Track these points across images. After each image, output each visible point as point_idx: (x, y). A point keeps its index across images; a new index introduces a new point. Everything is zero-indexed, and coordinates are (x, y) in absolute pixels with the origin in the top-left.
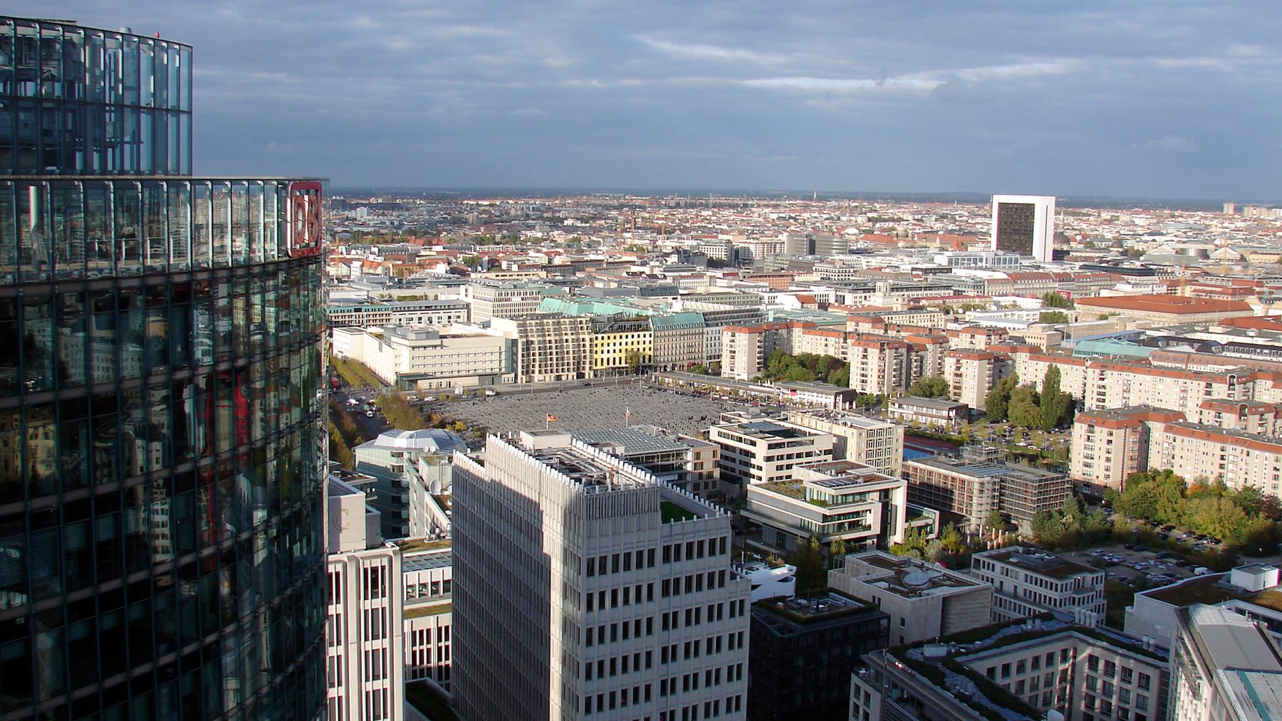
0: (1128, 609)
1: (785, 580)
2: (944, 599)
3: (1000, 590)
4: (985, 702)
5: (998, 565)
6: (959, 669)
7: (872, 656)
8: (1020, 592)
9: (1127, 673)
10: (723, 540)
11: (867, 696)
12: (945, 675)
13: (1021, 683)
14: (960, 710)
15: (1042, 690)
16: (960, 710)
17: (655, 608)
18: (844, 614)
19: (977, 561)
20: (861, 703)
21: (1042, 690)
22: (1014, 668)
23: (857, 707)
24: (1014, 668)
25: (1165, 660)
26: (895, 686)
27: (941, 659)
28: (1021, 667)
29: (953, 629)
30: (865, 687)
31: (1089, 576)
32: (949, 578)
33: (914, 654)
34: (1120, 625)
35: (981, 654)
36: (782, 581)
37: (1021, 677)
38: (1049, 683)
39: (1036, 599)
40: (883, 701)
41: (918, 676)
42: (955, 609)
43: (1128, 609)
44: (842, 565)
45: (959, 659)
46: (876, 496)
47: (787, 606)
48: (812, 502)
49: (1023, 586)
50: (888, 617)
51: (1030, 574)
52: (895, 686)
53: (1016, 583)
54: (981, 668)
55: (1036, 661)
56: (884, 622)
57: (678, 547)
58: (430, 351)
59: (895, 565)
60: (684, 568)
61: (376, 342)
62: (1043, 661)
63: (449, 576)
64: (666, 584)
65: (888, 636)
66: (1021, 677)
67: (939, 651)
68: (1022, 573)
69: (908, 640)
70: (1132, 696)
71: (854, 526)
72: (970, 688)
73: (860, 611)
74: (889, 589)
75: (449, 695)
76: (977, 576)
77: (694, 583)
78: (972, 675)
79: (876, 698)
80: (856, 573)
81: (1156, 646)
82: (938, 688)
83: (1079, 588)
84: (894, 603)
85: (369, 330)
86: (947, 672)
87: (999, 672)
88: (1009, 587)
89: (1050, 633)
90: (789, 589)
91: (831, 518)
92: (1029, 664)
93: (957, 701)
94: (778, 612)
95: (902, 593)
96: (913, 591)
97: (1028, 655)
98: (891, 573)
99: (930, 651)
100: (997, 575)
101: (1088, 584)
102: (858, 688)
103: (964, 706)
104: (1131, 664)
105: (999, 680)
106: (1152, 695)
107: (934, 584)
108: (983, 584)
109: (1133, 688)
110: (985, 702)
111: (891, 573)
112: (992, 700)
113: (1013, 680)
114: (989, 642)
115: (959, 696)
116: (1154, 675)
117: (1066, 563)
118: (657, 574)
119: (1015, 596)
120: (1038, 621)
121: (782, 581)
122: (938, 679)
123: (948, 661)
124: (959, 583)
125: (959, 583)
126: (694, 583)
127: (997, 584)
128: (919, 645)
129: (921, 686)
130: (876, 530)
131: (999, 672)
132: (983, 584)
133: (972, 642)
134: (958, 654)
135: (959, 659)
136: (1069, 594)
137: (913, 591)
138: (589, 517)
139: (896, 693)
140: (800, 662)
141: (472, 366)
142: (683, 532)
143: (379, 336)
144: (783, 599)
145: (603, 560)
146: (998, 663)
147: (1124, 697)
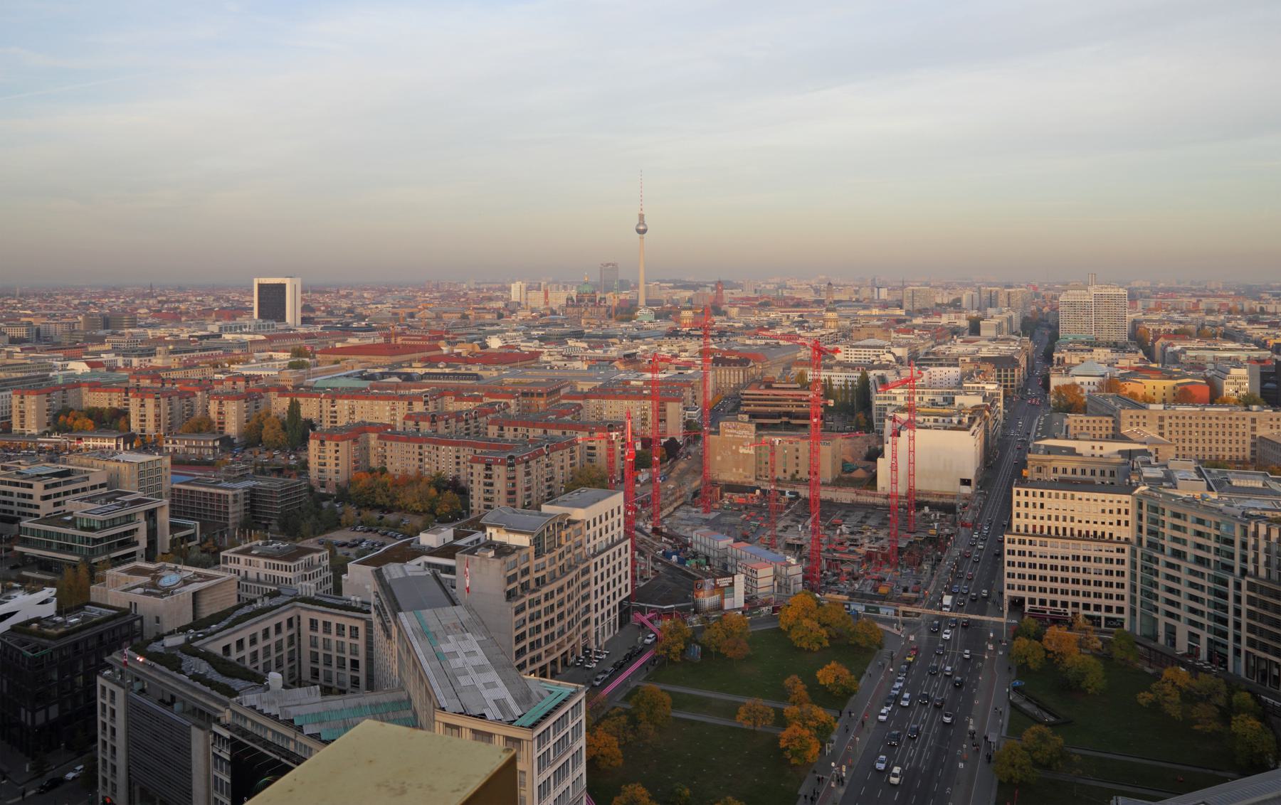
0: (344, 576)
2: (195, 595)
3: (246, 578)
4: (217, 677)
5: (243, 558)
6: (195, 653)
7: (116, 656)
8: (262, 577)
9: (340, 628)
11: (113, 693)
12: (181, 660)
13: (255, 655)
14: (195, 689)
15: (274, 655)
16: (195, 689)
18: (97, 623)
19: (225, 557)
20: (107, 702)
21: (274, 655)
22: (247, 642)
24: (247, 642)
25: (368, 612)
26: (138, 680)
27: (182, 648)
28: (253, 641)
30: (109, 686)
31: (316, 556)
32: (199, 575)
33: (156, 647)
34: (338, 589)
35: (217, 635)
36: (42, 603)
37: (255, 648)
39: (275, 580)
40: (126, 695)
41: (158, 666)
43: (344, 576)
44: (103, 579)
45: (196, 644)
46: (141, 517)
47: (41, 626)
48: (83, 529)
50: (141, 618)
51: (268, 561)
52: (138, 680)
53: (258, 570)
54: (216, 648)
56: (138, 623)
59: (152, 571)
65: (141, 634)
66: (255, 648)
67: (180, 640)
68: (262, 561)
71: (123, 544)
72: (204, 667)
73: (114, 617)
74: (145, 593)
76: (225, 570)
78: (207, 656)
79: (120, 693)
80: (116, 584)
81: (363, 602)
82: (174, 674)
84: (148, 605)
86: (184, 657)
87: (233, 648)
89: (278, 607)
90: (50, 609)
91: (101, 540)
93: (191, 682)
94: (32, 633)
95: (155, 595)
96: (168, 591)
97: (258, 629)
98: (147, 579)
99: (169, 642)
100: (242, 567)
101: (316, 562)
102: (104, 688)
103: (198, 684)
105: (234, 656)
106: (361, 642)
107: (186, 582)
108: (228, 576)
109: (347, 639)
110: (217, 677)
111: (147, 579)
112: (224, 674)
113: (248, 650)
114: (225, 623)
115: (196, 677)
116: (361, 625)
117: (298, 548)
119: (258, 581)
120: (266, 599)
121: (42, 603)
123: (188, 649)
124: (208, 578)
125: (208, 578)
127: (242, 573)
128: (159, 638)
130: (143, 543)
131: (233, 648)
132: (228, 576)
133: (208, 627)
134: (196, 639)
135: (196, 644)
136: (301, 572)
139: (137, 686)
140: (55, 676)
144: (38, 620)
146: (232, 640)
147: (341, 648)
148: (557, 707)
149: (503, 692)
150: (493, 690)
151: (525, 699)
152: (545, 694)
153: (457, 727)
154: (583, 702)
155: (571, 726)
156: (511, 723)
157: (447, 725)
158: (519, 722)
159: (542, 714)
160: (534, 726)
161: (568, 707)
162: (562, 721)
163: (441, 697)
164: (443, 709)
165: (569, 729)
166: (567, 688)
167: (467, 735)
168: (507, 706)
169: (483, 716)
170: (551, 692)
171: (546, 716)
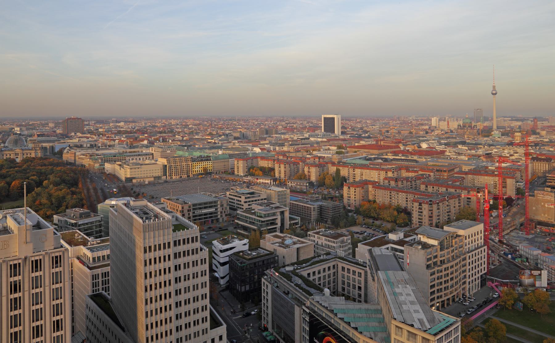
0: (356, 249)
1: (245, 244)
2: (298, 249)
3: (317, 244)
5: (316, 236)
6: (297, 275)
7: (268, 271)
8: (324, 245)
9: (354, 272)
10: (197, 237)
11: (267, 286)
12: (292, 277)
13: (320, 278)
14: (296, 290)
15: (327, 279)
16: (296, 290)
17: (171, 264)
18: (262, 256)
19: (309, 235)
20: (265, 288)
21: (327, 279)
22: (317, 273)
23: (264, 290)
24: (317, 273)
25: (366, 267)
27: (291, 271)
28: (319, 273)
29: (301, 259)
30: (266, 283)
31: (345, 238)
32: (300, 241)
33: (282, 270)
34: (354, 256)
35: (305, 268)
37: (319, 276)
38: (329, 277)
39: (329, 247)
40: (272, 287)
41: (283, 278)
42: (301, 251)
43: (356, 249)
44: (264, 238)
46: (279, 214)
47: (243, 254)
48: (258, 216)
49: (325, 242)
50: (278, 256)
53: (322, 241)
54: (305, 274)
55: (324, 270)
56: (276, 258)
57: (179, 241)
58: (137, 170)
60: (181, 248)
61: (119, 167)
62: (327, 269)
63: (109, 253)
64: (175, 254)
65: (278, 263)
66: (319, 276)
67: (290, 268)
68: (324, 238)
69: (287, 263)
70: (357, 280)
71: (272, 224)
72: (300, 281)
74: (279, 246)
75: (109, 297)
76: (309, 240)
77: (186, 253)
78: (301, 277)
80: (269, 241)
81: (363, 262)
82: (289, 282)
83: (342, 242)
84: (281, 251)
85: (117, 163)
86: (293, 276)
87: (311, 274)
88: (320, 243)
89: (329, 260)
90: (246, 248)
91: (264, 221)
92: (322, 271)
93: (295, 287)
94: (240, 256)
95: (283, 247)
96: (287, 246)
97: (321, 268)
98: (280, 240)
99: (288, 269)
100: (316, 239)
101: (345, 241)
102: (264, 283)
103: (297, 288)
104: (355, 269)
105: (311, 278)
106: (362, 279)
107: (295, 243)
108: (311, 243)
109: (357, 277)
111: (280, 240)
113: (317, 276)
114: (308, 264)
115: (297, 285)
116: (363, 272)
117: (338, 234)
118: (171, 251)
119: (322, 246)
120: (325, 256)
122: (289, 278)
123: (294, 272)
124: (303, 242)
125: (303, 242)
126: (186, 253)
127: (316, 242)
128: (284, 267)
129: (284, 281)
131: (311, 274)
133: (302, 264)
134: (297, 269)
136: (339, 244)
137: (287, 246)
138: (144, 232)
139: (276, 285)
140: (248, 274)
141: (151, 175)
142: (181, 235)
143: (120, 165)
144: (242, 252)
145: (179, 241)
146: (311, 271)
147: (354, 280)
148: (447, 327)
149: (422, 316)
150: (418, 314)
151: (432, 320)
152: (442, 320)
153: (401, 328)
154: (460, 327)
155: (453, 337)
156: (425, 331)
157: (397, 326)
158: (429, 331)
159: (439, 329)
160: (435, 335)
161: (452, 328)
162: (448, 335)
163: (394, 313)
164: (395, 319)
165: (452, 338)
166: (452, 319)
167: (405, 333)
168: (424, 323)
169: (412, 326)
170: (444, 320)
171: (442, 331)
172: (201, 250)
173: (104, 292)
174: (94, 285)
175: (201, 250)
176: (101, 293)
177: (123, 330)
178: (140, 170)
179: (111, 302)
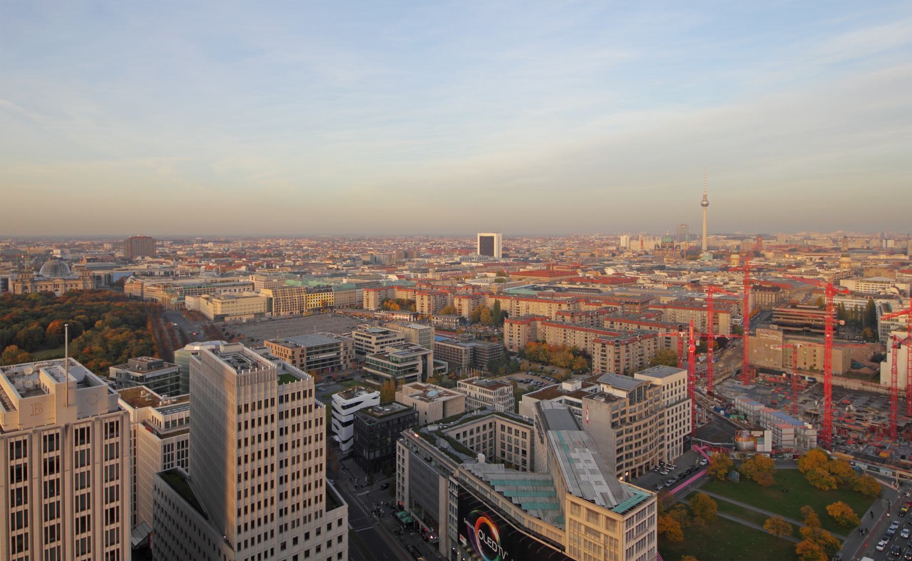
1: (375, 398)
2: (444, 403)
3: (469, 396)
4: (452, 451)
5: (468, 385)
7: (404, 432)
9: (517, 432)
10: (310, 391)
14: (442, 456)
15: (482, 441)
16: (442, 456)
18: (397, 413)
21: (482, 441)
22: (468, 433)
24: (468, 433)
25: (532, 425)
28: (472, 433)
29: (449, 415)
30: (402, 447)
31: (506, 388)
33: (424, 430)
34: (517, 411)
37: (472, 437)
38: (484, 438)
39: (484, 399)
42: (449, 406)
44: (401, 389)
45: (443, 431)
46: (420, 358)
47: (373, 411)
49: (479, 394)
54: (452, 434)
55: (478, 429)
58: (231, 305)
62: (481, 428)
63: (188, 415)
66: (472, 437)
68: (478, 388)
69: (429, 422)
70: (520, 442)
71: (412, 371)
72: (445, 444)
73: (405, 410)
75: (187, 474)
76: (459, 391)
78: (448, 439)
80: (407, 393)
83: (502, 393)
84: (422, 406)
88: (473, 395)
90: (377, 402)
92: (475, 431)
94: (368, 414)
96: (431, 399)
97: (474, 427)
99: (430, 428)
100: (468, 390)
104: (518, 428)
105: (461, 440)
106: (528, 441)
107: (440, 395)
108: (461, 394)
109: (520, 438)
110: (452, 451)
111: (420, 392)
112: (456, 450)
113: (469, 437)
114: (457, 422)
115: (442, 449)
116: (528, 432)
119: (476, 398)
122: (432, 441)
123: (439, 433)
124: (451, 394)
125: (451, 394)
128: (426, 426)
129: (426, 445)
130: (421, 372)
132: (461, 394)
134: (443, 428)
135: (443, 431)
136: (498, 396)
137: (431, 399)
138: (238, 386)
139: (415, 449)
140: (378, 436)
141: (251, 311)
142: (290, 388)
143: (207, 299)
144: (371, 407)
145: (287, 396)
146: (461, 431)
147: (517, 442)
148: (639, 504)
149: (606, 489)
150: (601, 487)
151: (619, 495)
152: (632, 494)
153: (578, 505)
154: (656, 504)
155: (647, 517)
156: (610, 509)
157: (572, 503)
159: (629, 507)
160: (624, 514)
162: (641, 514)
163: (569, 485)
166: (646, 493)
167: (584, 512)
168: (608, 498)
169: (593, 502)
172: (316, 407)
173: (180, 468)
174: (166, 459)
175: (316, 407)
176: (176, 469)
177: (206, 517)
178: (235, 304)
179: (190, 480)
